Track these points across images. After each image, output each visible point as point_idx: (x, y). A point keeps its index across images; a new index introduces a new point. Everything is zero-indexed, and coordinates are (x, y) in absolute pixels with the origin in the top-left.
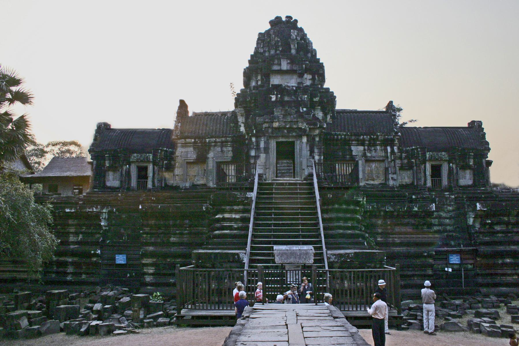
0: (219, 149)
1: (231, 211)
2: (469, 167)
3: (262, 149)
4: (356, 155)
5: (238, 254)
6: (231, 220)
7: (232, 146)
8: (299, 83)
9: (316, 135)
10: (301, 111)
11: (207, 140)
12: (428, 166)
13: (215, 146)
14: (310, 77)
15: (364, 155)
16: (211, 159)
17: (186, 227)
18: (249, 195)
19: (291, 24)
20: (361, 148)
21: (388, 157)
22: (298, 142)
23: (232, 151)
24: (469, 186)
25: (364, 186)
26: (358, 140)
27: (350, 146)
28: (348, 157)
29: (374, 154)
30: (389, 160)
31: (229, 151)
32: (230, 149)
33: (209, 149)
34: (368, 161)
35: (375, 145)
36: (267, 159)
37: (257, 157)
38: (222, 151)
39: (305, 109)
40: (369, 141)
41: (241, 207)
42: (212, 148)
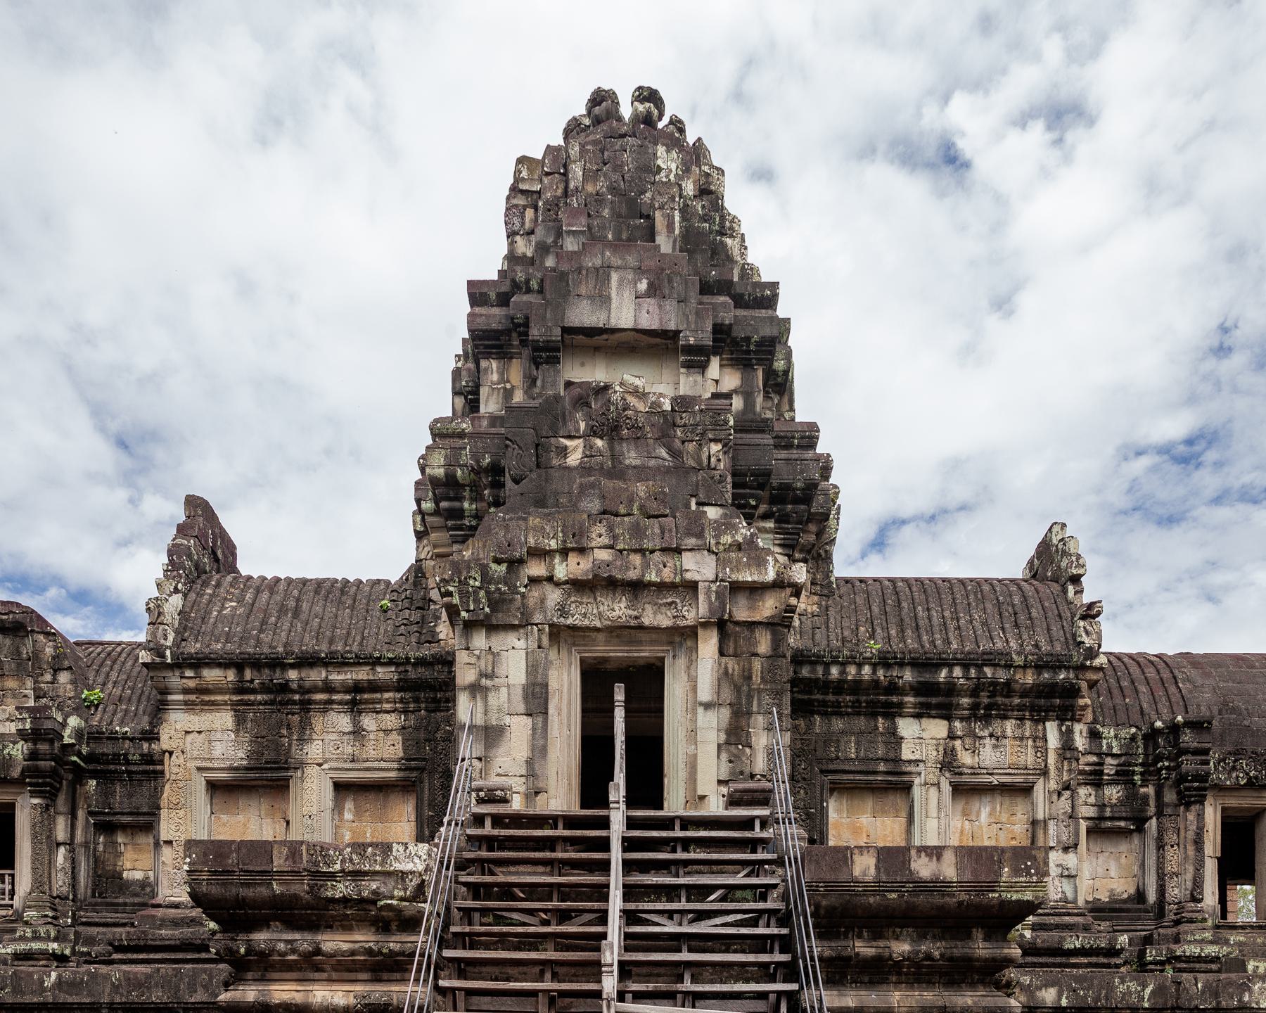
0: (343, 722)
4: (917, 762)
12: (1212, 815)
13: (327, 706)
20: (937, 729)
21: (1045, 773)
30: (1053, 785)
31: (387, 732)
33: (305, 724)
38: (358, 733)
41: (364, 938)
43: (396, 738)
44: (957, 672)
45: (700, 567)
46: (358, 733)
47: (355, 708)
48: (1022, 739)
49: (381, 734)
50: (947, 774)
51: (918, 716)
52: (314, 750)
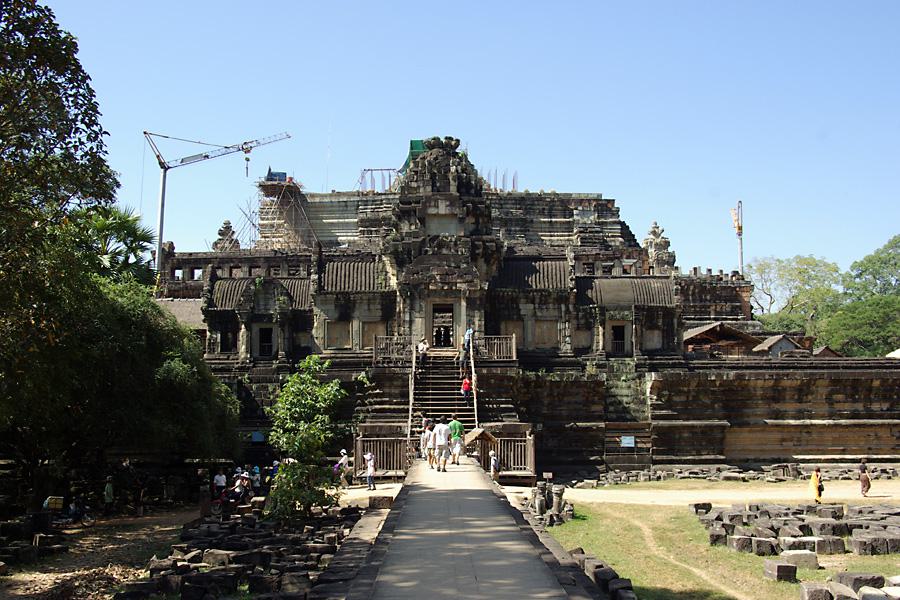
1: (390, 387)
2: (658, 328)
5: (400, 427)
7: (382, 305)
15: (535, 314)
18: (408, 370)
19: (448, 148)
20: (531, 306)
24: (657, 350)
26: (527, 298)
32: (379, 307)
34: (537, 320)
35: (546, 303)
38: (369, 309)
40: (540, 299)
42: (357, 305)
46: (369, 309)
52: (356, 313)
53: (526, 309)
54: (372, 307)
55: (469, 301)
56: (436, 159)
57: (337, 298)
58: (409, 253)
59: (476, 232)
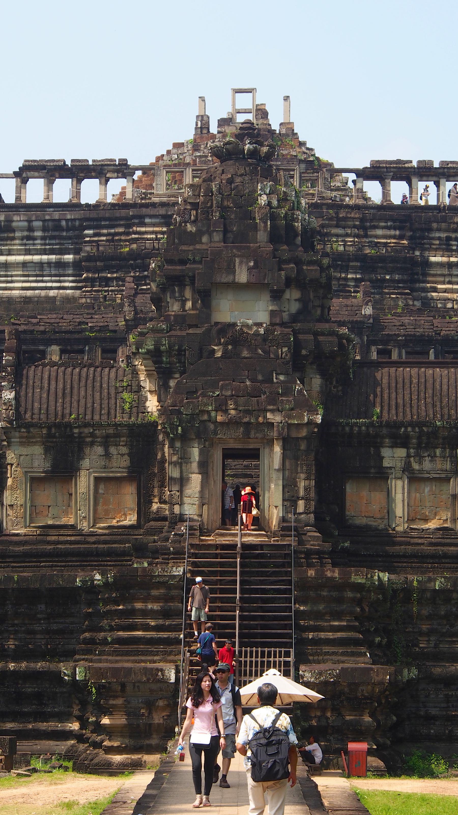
0: (100, 450)
3: (195, 466)
4: (390, 468)
6: (145, 613)
8: (273, 314)
9: (302, 438)
10: (275, 380)
11: (76, 431)
13: (92, 444)
14: (296, 294)
15: (407, 468)
16: (83, 473)
17: (40, 619)
20: (401, 452)
22: (267, 450)
23: (129, 455)
25: (405, 532)
27: (378, 447)
28: (373, 470)
29: (427, 465)
31: (122, 455)
36: (204, 484)
37: (183, 481)
38: (107, 455)
39: (282, 378)
40: (419, 438)
43: (126, 457)
44: (409, 429)
45: (275, 418)
46: (107, 455)
47: (106, 445)
48: (444, 457)
49: (119, 456)
50: (406, 473)
51: (392, 447)
52: (86, 463)
53: (392, 457)
54: (113, 450)
55: (288, 443)
56: (230, 181)
57: (49, 435)
58: (181, 352)
59: (303, 314)
